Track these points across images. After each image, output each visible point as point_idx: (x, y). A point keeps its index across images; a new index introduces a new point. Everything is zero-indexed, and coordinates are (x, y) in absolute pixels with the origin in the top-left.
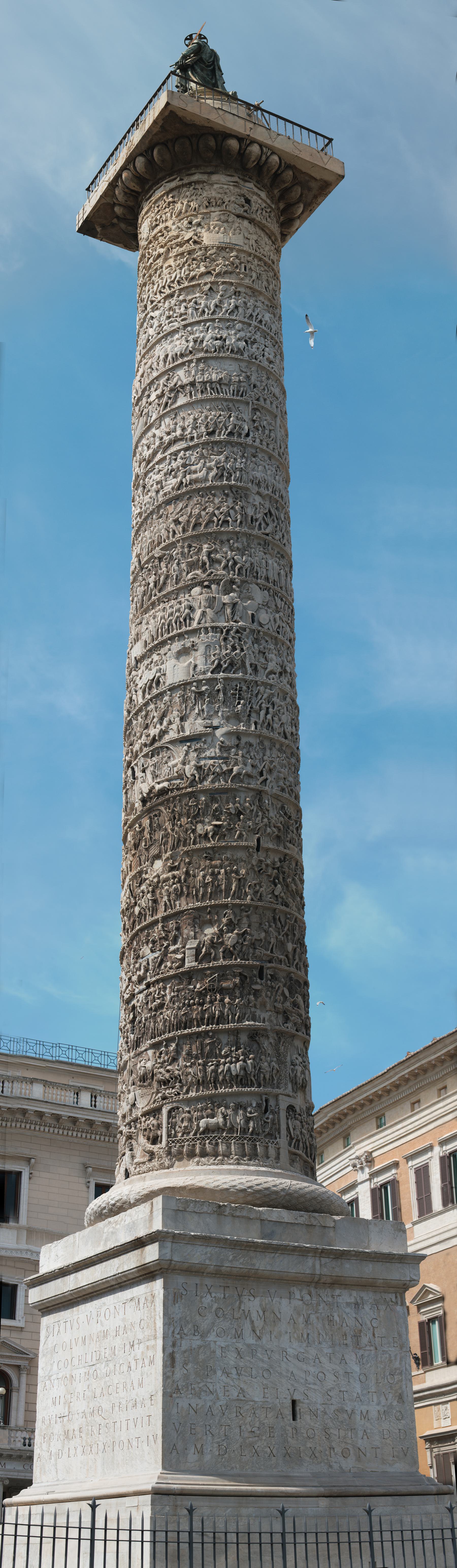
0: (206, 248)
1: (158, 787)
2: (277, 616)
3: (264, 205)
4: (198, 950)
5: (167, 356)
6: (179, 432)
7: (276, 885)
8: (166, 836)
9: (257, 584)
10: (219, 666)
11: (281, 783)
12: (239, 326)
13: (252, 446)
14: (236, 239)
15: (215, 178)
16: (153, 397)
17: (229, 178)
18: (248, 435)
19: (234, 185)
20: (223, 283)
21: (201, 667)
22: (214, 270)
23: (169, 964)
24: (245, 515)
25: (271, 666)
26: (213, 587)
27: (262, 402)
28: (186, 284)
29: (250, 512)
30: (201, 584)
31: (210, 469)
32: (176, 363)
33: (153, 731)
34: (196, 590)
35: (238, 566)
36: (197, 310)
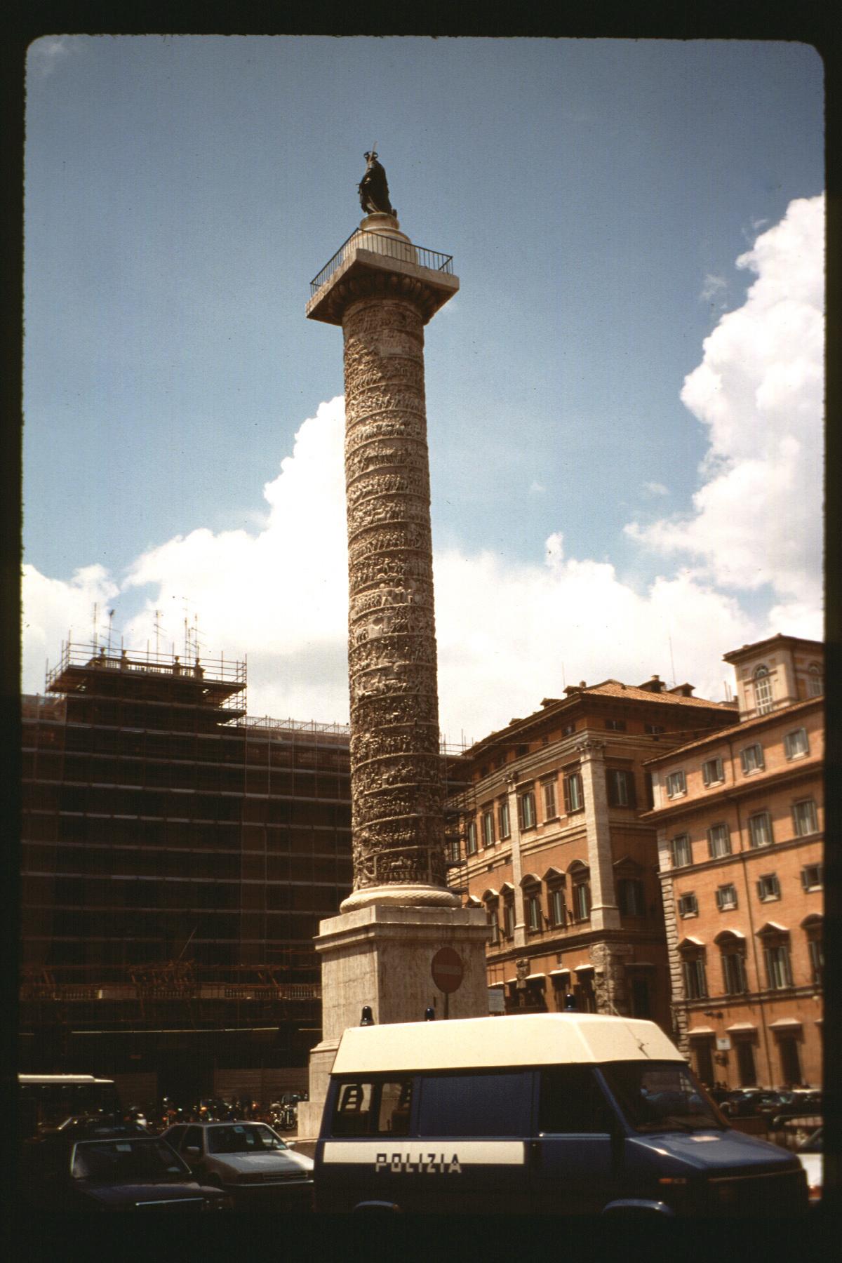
0: (381, 359)
1: (367, 694)
2: (424, 594)
3: (414, 316)
4: (388, 779)
5: (362, 435)
6: (370, 487)
7: (424, 742)
8: (371, 720)
9: (413, 579)
10: (395, 628)
11: (427, 689)
12: (401, 414)
13: (409, 495)
14: (398, 350)
15: (384, 302)
16: (356, 460)
17: (394, 302)
18: (407, 488)
19: (396, 307)
20: (392, 385)
21: (385, 630)
22: (386, 375)
23: (375, 785)
24: (406, 539)
25: (421, 624)
26: (391, 584)
27: (414, 465)
28: (371, 386)
29: (409, 537)
30: (384, 582)
31: (387, 512)
32: (368, 442)
33: (363, 663)
34: (382, 585)
35: (403, 570)
36: (377, 404)
